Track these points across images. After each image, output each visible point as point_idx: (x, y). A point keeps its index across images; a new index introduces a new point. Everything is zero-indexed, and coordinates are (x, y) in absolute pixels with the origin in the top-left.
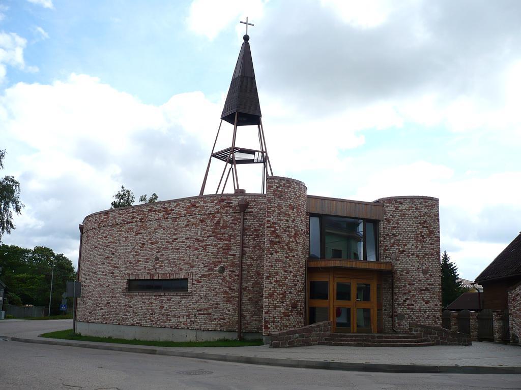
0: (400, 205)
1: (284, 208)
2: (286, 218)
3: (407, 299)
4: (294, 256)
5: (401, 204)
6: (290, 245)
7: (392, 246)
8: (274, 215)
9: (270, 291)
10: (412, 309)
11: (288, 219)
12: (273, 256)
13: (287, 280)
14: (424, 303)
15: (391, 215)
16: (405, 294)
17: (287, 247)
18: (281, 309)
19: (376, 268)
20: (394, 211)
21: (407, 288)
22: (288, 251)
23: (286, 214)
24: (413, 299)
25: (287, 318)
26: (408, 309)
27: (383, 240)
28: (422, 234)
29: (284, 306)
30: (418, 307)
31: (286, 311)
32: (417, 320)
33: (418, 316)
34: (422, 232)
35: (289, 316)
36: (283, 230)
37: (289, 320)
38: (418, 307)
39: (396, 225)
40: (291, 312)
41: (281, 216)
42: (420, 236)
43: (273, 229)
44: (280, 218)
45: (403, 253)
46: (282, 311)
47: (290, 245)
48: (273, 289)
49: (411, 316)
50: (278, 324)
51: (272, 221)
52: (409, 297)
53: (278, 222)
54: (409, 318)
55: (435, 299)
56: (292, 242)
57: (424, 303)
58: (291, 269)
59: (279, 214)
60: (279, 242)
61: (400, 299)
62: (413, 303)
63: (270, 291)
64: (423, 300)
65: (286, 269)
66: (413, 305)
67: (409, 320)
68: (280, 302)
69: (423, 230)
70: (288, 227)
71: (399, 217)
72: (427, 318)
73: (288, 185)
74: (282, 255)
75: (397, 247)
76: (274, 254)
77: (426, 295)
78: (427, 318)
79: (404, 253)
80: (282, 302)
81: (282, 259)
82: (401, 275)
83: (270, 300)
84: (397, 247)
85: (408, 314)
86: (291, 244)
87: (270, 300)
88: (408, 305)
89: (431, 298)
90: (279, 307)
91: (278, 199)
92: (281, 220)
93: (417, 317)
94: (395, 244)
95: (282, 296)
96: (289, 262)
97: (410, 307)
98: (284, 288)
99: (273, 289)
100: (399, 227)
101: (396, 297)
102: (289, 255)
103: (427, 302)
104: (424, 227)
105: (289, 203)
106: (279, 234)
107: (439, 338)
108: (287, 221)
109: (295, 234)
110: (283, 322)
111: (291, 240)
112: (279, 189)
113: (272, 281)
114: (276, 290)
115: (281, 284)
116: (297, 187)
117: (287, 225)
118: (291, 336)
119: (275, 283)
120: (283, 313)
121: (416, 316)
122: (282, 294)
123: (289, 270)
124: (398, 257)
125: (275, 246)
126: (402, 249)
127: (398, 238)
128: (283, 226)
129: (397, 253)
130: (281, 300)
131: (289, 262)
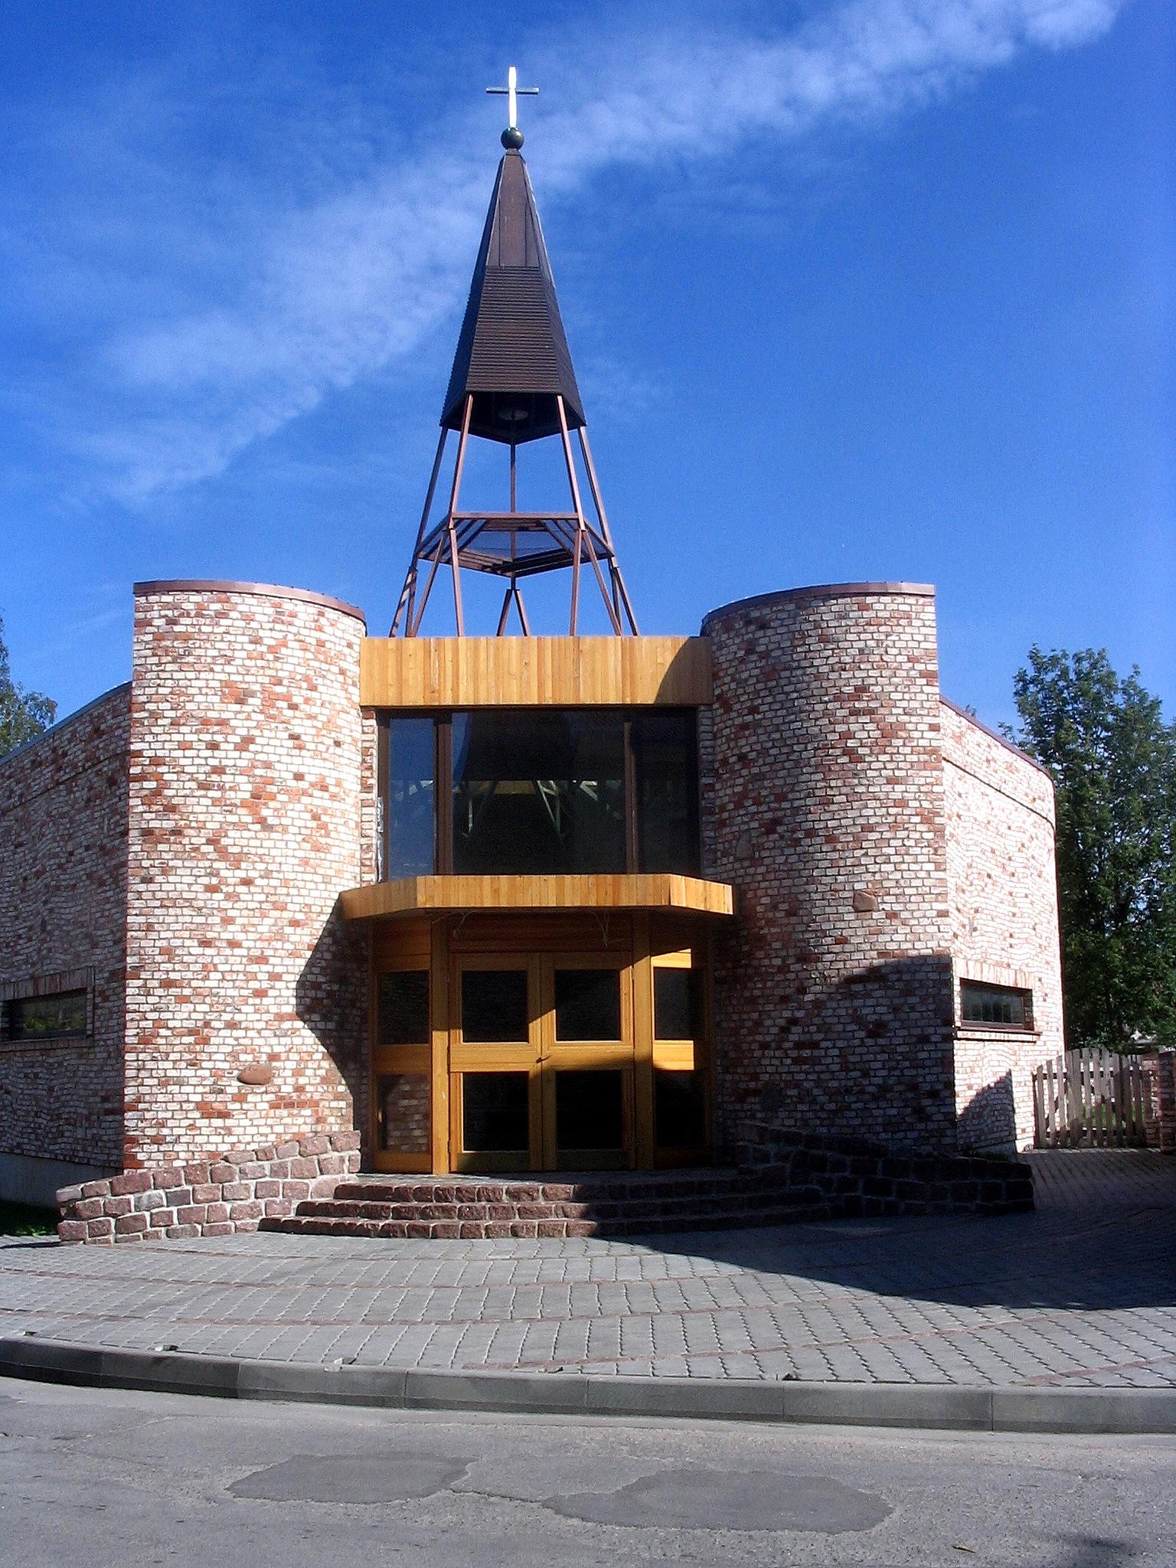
0: (760, 634)
1: (198, 698)
2: (207, 737)
3: (794, 1021)
4: (247, 882)
5: (763, 626)
6: (224, 841)
7: (739, 805)
8: (155, 730)
9: (143, 1024)
10: (814, 1061)
11: (218, 738)
12: (152, 887)
13: (212, 975)
14: (863, 1034)
15: (733, 680)
16: (785, 999)
17: (211, 848)
18: (190, 1089)
19: (593, 904)
20: (742, 661)
21: (792, 976)
22: (216, 865)
23: (206, 722)
24: (816, 1021)
25: (218, 1122)
26: (797, 1061)
27: (712, 785)
28: (851, 743)
29: (204, 1078)
30: (836, 1052)
31: (211, 1098)
32: (832, 1106)
33: (838, 1092)
34: (849, 735)
35: (224, 1115)
36: (194, 785)
37: (229, 1131)
38: (836, 1052)
39: (749, 718)
40: (240, 1098)
41: (183, 729)
42: (838, 752)
43: (153, 785)
44: (179, 737)
45: (774, 832)
46: (192, 1098)
47: (224, 841)
48: (154, 1016)
49: (808, 1092)
50: (177, 1148)
51: (151, 753)
52: (800, 1014)
53: (175, 754)
54: (801, 1101)
55: (913, 1015)
56: (240, 826)
57: (863, 1034)
58: (233, 932)
59: (174, 723)
60: (177, 832)
61: (768, 1023)
62: (818, 1037)
63: (143, 1024)
64: (858, 1019)
65: (210, 935)
66: (814, 1045)
67: (800, 1107)
68: (183, 1065)
69: (853, 727)
70: (219, 770)
71: (758, 682)
72: (875, 1098)
73: (217, 606)
74: (191, 880)
75: (753, 809)
76: (159, 879)
77: (870, 1002)
78: (875, 1098)
79: (780, 829)
80: (193, 1064)
81: (192, 895)
82: (771, 923)
83: (142, 1056)
84: (753, 809)
85: (797, 1085)
86: (231, 834)
87: (142, 1056)
88: (799, 1045)
89: (895, 1010)
90: (180, 1082)
91: (175, 667)
92: (184, 746)
93: (832, 1094)
94: (747, 798)
95: (191, 1039)
96: (225, 905)
97: (806, 1053)
98: (199, 1008)
99: (154, 1016)
100: (757, 724)
101: (755, 1015)
102: (223, 881)
103: (877, 1030)
104: (855, 712)
105: (223, 677)
106: (175, 801)
107: (860, 1185)
108: (213, 746)
109: (255, 796)
110: (198, 1139)
111: (231, 818)
112: (177, 628)
113: (150, 984)
114: (164, 1016)
115: (187, 992)
116: (732, 647)
117: (211, 762)
118: (132, 1197)
119: (160, 992)
120: (199, 1106)
121: (826, 1091)
122: (191, 1032)
123: (224, 936)
124: (760, 847)
125: (161, 847)
126: (769, 815)
127: (755, 770)
128: (193, 769)
129: (754, 834)
130: (187, 1056)
131: (225, 905)
